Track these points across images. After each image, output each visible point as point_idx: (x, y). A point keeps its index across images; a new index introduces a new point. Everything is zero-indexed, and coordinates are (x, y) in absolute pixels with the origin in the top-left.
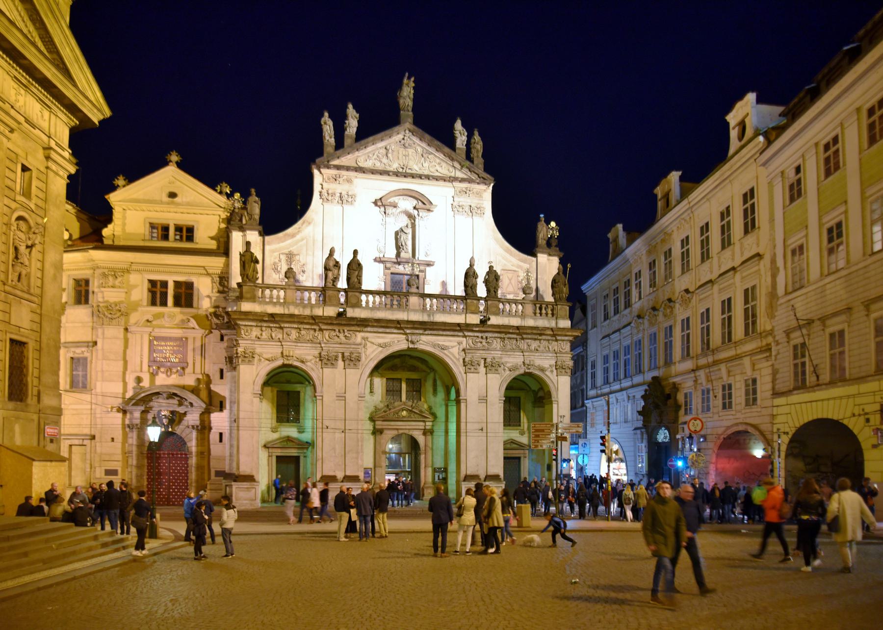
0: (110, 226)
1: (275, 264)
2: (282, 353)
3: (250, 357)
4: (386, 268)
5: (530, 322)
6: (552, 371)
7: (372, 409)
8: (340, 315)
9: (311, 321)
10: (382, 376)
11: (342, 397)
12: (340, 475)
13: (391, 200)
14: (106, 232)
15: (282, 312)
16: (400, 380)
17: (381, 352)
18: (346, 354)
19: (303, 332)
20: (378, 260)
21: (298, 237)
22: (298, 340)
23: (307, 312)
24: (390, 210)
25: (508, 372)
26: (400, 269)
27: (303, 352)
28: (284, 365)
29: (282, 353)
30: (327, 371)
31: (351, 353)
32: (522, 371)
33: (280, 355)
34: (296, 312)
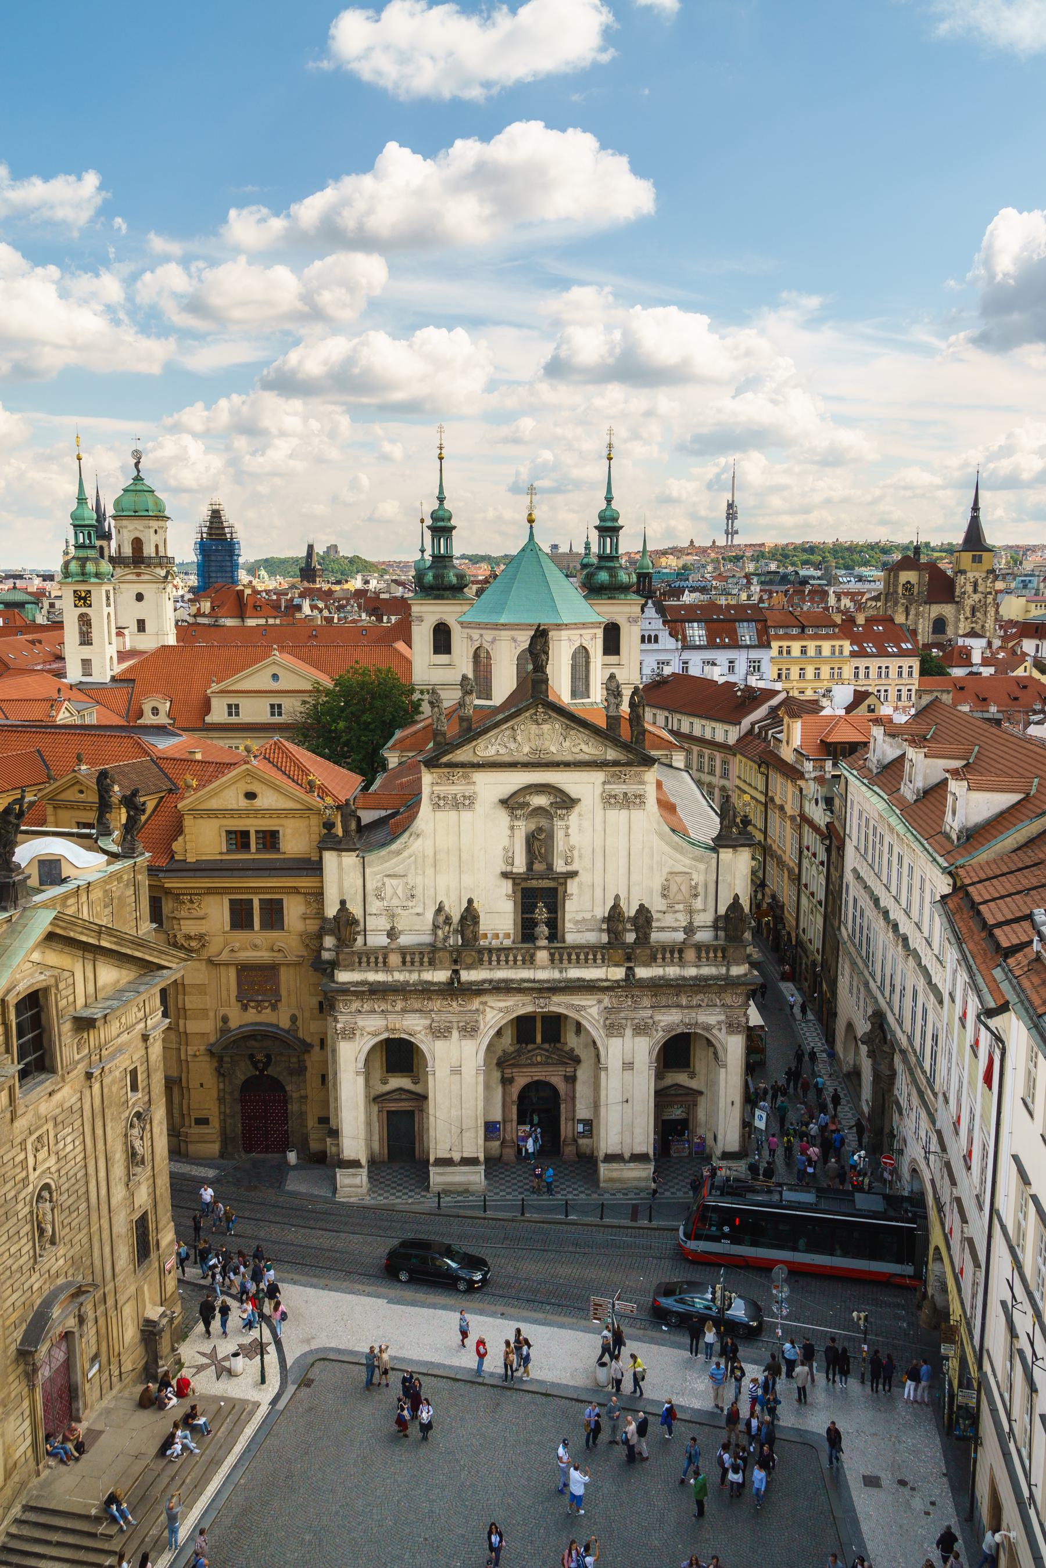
0: (180, 839)
1: (377, 888)
3: (350, 1034)
4: (514, 884)
5: (691, 972)
6: (720, 1030)
11: (456, 1071)
13: (522, 800)
14: (177, 846)
17: (503, 1018)
20: (505, 875)
21: (405, 854)
22: (404, 1011)
24: (519, 812)
25: (661, 1033)
26: (534, 884)
27: (413, 1025)
30: (440, 1045)
32: (679, 1031)
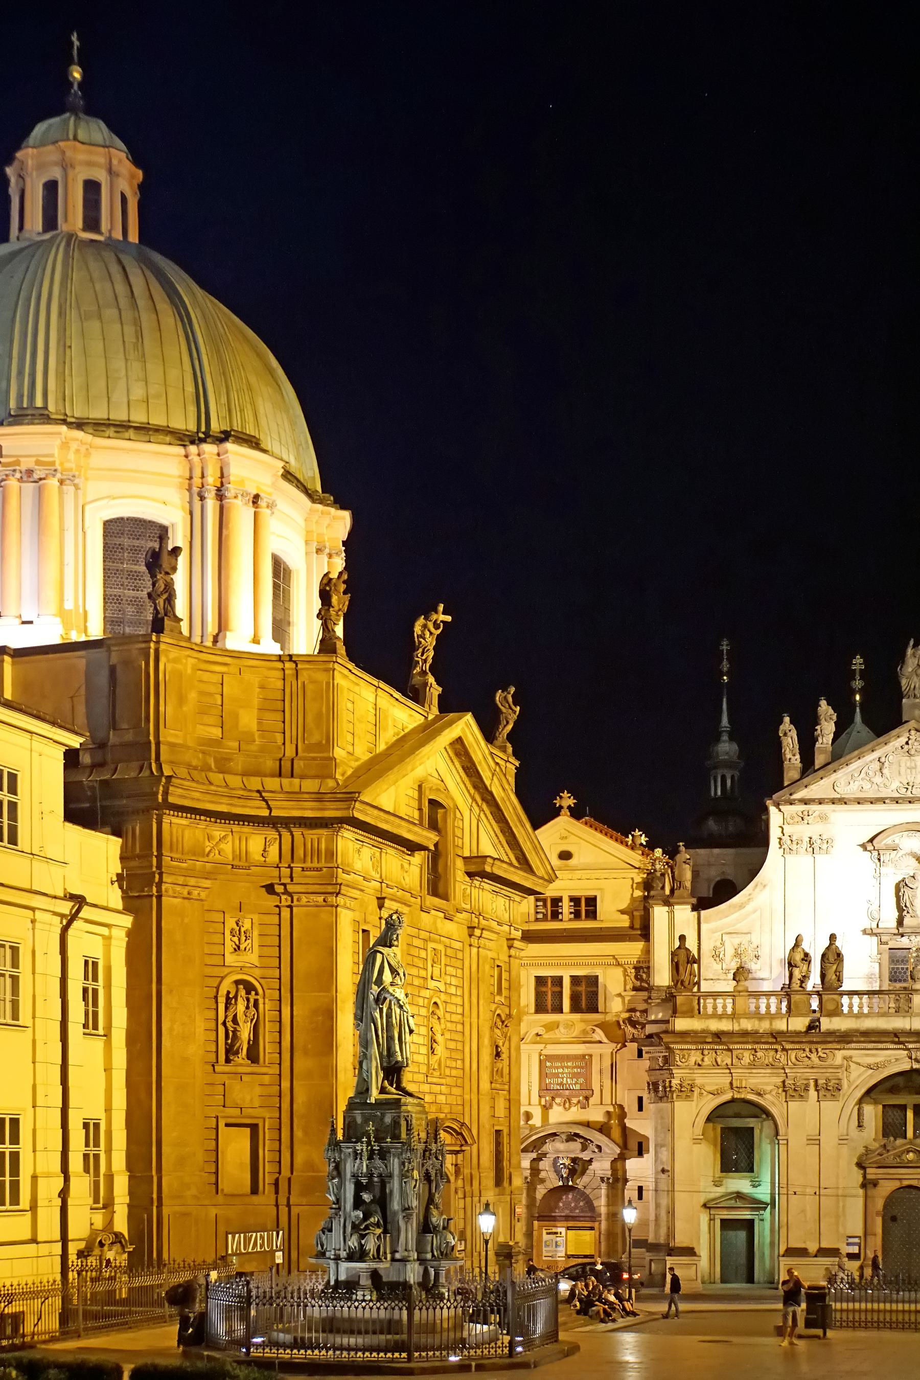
2: (731, 1084)
7: (862, 1150)
8: (810, 1027)
9: (771, 1040)
10: (876, 1102)
11: (815, 1141)
12: (813, 1248)
15: (730, 1028)
16: (904, 1108)
17: (871, 1076)
18: (820, 1082)
19: (760, 1054)
22: (752, 1065)
23: (764, 1026)
27: (761, 1084)
28: (733, 1100)
29: (731, 1084)
31: (828, 1080)
33: (728, 1085)
34: (749, 1028)
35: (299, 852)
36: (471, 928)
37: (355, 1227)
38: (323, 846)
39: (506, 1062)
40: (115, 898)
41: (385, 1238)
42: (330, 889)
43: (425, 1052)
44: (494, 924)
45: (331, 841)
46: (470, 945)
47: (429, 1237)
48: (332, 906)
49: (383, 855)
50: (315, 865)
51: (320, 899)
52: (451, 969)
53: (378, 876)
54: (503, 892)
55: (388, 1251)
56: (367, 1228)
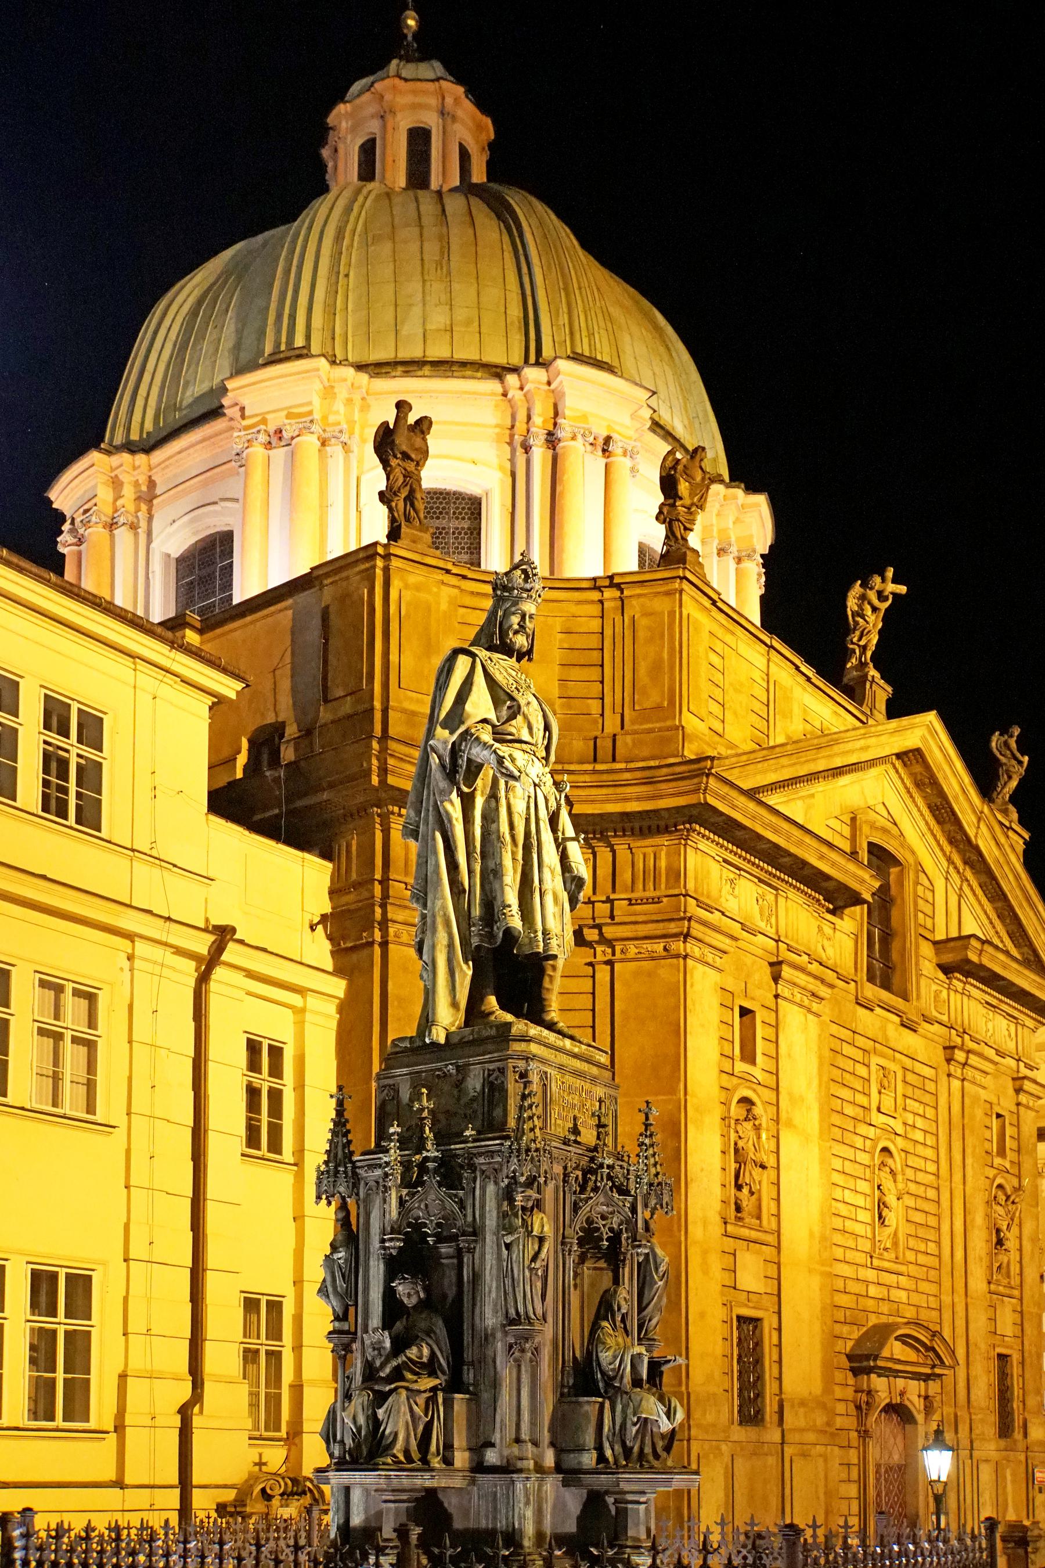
35: (625, 876)
36: (949, 1049)
37: (370, 1374)
38: (663, 864)
39: (1014, 1256)
40: (319, 949)
41: (448, 1404)
42: (673, 928)
43: (868, 1220)
44: (991, 1053)
45: (675, 854)
46: (949, 1075)
47: (590, 1405)
48: (678, 956)
49: (781, 901)
50: (651, 893)
51: (659, 947)
52: (917, 1104)
53: (773, 930)
54: (1004, 1007)
55: (459, 1440)
56: (397, 1375)
